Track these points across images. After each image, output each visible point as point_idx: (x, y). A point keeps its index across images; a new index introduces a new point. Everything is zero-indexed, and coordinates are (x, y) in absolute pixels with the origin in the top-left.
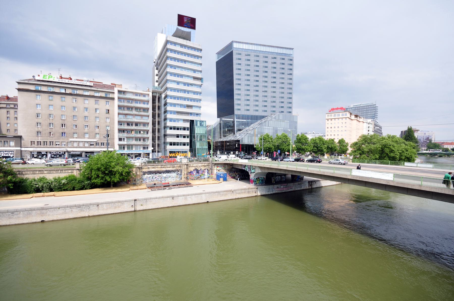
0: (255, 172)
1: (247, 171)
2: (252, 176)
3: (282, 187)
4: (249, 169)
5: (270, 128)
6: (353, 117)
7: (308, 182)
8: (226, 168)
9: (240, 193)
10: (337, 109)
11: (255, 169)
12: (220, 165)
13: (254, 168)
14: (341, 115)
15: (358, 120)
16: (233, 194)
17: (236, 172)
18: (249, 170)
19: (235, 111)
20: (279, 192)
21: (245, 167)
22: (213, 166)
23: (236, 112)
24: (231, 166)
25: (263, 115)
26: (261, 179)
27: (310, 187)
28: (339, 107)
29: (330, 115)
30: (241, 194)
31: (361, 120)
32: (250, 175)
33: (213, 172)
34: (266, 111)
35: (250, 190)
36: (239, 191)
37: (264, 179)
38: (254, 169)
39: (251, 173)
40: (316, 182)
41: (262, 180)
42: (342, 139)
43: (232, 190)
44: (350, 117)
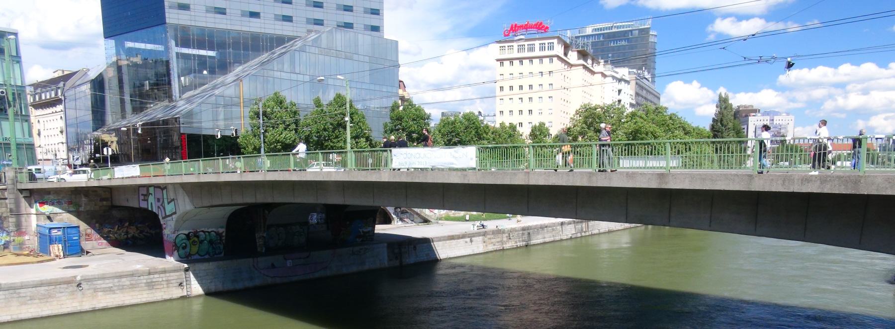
0: (175, 213)
1: (155, 213)
2: (169, 231)
3: (288, 265)
4: (159, 204)
5: (300, 78)
6: (573, 57)
7: (386, 245)
8: (82, 209)
9: (110, 291)
11: (176, 201)
12: (52, 197)
13: (172, 198)
14: (537, 47)
15: (590, 66)
16: (80, 293)
17: (130, 225)
18: (159, 207)
19: (167, 10)
20: (278, 280)
21: (146, 198)
22: (24, 203)
23: (172, 17)
24: (102, 200)
25: (279, 32)
26: (208, 238)
27: (396, 263)
28: (533, 22)
29: (507, 48)
30: (118, 292)
31: (599, 68)
32: (164, 226)
33: (24, 224)
34: (288, 19)
35: (156, 276)
36: (107, 281)
37: (221, 240)
39: (166, 216)
40: (415, 247)
41: (211, 242)
42: (542, 125)
43: (75, 277)
44: (566, 54)
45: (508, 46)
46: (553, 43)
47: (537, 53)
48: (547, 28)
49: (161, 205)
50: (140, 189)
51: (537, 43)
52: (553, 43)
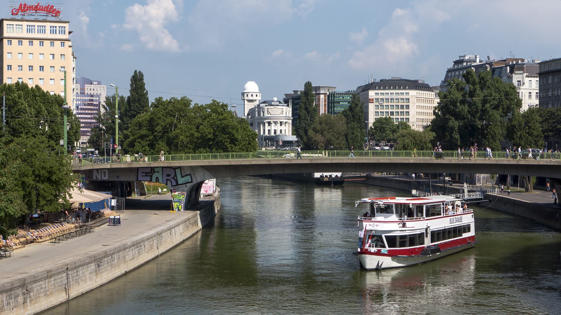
0: (192, 182)
4: (168, 178)
10: (36, 8)
13: (188, 173)
14: (48, 29)
18: (167, 180)
28: (43, 4)
29: (15, 26)
38: (190, 175)
45: (16, 25)
46: (64, 27)
47: (48, 35)
48: (59, 12)
49: (173, 178)
50: (155, 168)
51: (48, 25)
52: (64, 27)
